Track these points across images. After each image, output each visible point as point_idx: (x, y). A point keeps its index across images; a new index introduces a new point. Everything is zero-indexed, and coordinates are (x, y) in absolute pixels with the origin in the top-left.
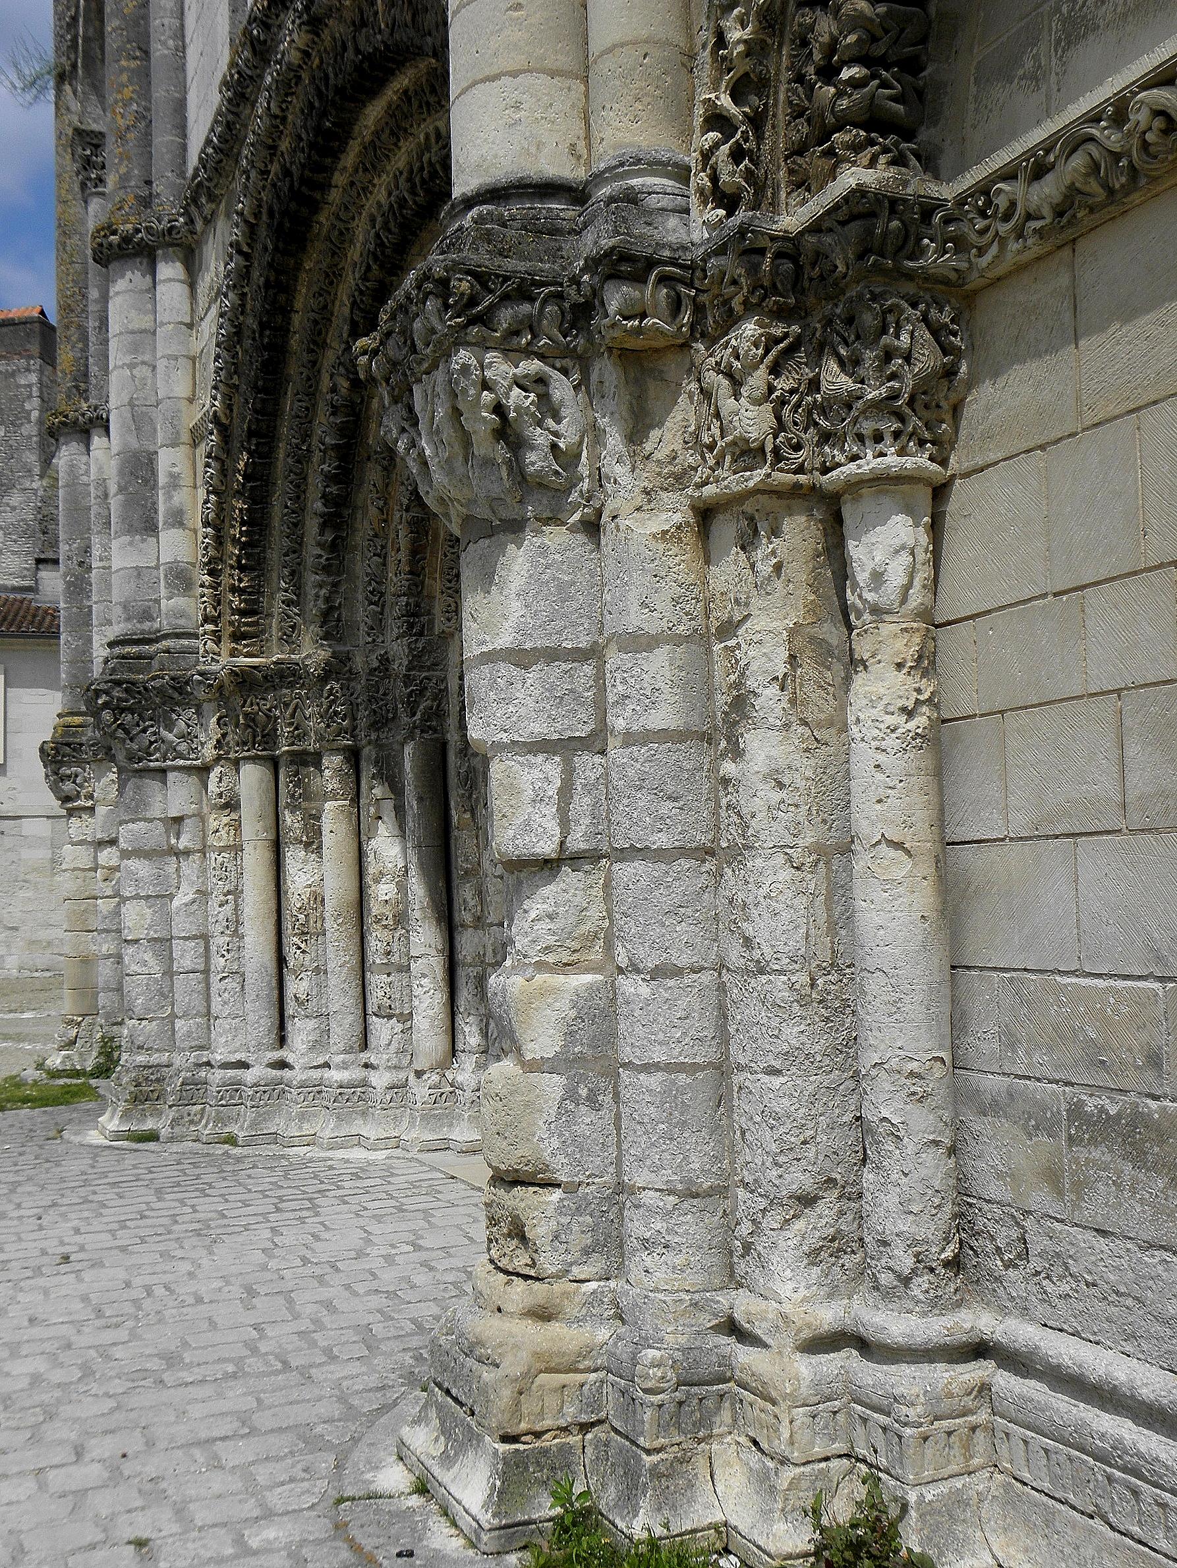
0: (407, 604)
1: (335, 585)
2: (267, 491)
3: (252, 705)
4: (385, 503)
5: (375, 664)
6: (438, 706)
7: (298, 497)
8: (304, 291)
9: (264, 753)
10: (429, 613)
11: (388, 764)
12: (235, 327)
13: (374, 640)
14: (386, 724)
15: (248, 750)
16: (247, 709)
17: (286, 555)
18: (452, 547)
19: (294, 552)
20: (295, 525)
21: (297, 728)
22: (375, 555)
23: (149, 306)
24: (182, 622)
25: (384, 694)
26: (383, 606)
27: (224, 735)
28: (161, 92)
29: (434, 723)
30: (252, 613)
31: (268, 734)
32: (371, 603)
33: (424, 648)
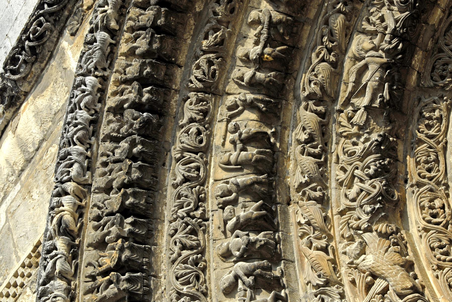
2: (148, 286)
8: (189, 41)
12: (92, 115)
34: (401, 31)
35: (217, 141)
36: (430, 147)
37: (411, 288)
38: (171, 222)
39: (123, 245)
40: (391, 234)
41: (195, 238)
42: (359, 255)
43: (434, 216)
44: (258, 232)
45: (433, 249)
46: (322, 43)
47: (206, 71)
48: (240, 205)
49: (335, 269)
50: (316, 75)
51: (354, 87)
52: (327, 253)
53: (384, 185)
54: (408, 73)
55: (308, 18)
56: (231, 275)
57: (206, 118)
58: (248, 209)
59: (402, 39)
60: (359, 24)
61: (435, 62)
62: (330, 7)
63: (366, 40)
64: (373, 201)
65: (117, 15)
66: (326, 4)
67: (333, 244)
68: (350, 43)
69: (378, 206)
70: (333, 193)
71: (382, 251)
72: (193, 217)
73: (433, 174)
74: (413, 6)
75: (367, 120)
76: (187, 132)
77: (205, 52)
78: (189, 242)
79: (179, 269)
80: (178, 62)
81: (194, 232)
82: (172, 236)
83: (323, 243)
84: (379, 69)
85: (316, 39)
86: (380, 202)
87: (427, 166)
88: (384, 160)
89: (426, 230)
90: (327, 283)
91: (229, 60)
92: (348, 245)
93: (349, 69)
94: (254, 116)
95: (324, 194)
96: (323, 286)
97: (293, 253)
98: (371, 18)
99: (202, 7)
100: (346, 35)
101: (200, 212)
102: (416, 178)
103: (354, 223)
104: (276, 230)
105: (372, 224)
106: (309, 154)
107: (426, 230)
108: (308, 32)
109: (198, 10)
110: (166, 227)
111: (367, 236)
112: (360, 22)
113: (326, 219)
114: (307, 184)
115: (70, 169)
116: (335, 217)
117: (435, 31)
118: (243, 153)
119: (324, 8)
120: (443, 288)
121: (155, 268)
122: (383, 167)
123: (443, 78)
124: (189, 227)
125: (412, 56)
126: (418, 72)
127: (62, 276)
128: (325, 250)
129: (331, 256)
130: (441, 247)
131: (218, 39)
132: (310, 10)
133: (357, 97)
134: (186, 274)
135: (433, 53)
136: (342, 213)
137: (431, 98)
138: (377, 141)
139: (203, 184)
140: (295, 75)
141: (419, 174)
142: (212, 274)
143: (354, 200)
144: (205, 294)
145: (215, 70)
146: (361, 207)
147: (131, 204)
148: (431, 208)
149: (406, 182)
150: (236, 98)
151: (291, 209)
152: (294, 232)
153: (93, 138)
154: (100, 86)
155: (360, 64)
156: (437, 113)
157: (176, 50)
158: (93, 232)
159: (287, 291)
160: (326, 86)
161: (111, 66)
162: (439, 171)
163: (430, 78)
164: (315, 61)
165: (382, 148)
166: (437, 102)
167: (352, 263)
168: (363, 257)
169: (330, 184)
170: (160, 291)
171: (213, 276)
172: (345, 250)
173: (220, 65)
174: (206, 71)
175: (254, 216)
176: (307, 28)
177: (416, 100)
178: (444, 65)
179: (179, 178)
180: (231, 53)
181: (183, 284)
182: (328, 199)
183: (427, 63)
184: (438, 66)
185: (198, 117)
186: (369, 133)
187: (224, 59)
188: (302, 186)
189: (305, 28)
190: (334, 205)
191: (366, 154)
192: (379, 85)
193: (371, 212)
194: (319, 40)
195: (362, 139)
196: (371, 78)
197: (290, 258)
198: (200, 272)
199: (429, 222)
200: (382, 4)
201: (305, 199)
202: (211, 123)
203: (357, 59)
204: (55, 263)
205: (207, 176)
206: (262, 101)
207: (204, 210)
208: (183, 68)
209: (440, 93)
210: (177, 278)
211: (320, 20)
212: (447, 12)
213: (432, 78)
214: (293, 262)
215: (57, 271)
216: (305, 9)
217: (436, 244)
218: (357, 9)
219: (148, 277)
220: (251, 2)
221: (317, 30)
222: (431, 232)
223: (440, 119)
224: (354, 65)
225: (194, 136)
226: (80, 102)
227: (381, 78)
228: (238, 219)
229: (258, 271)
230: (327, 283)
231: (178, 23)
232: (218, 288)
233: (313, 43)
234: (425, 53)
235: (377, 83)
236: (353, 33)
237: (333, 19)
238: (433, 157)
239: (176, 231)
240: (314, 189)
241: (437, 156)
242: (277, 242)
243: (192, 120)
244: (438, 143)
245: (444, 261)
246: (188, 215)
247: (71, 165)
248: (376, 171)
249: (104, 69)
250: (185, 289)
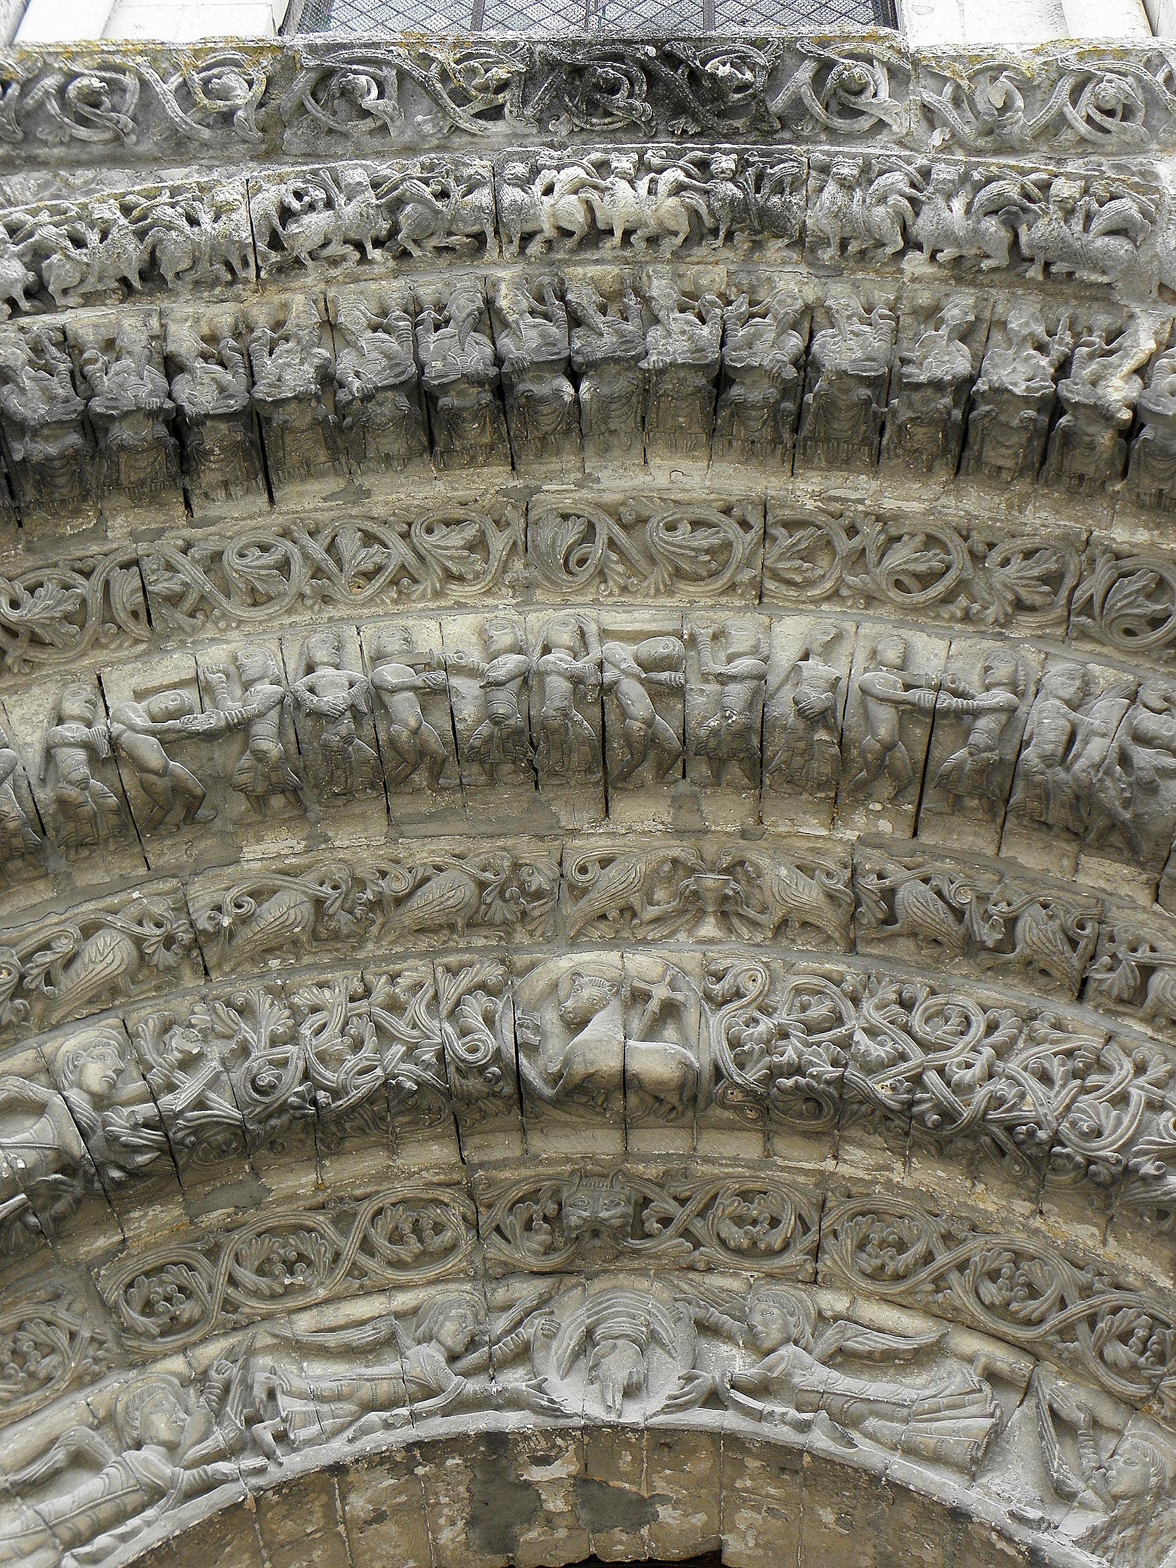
34: (180, 1134)
46: (26, 958)
54: (99, 1226)
55: (69, 876)
59: (168, 1149)
60: (143, 1013)
61: (175, 1264)
62: (134, 910)
63: (109, 1061)
66: (136, 895)
68: (81, 1024)
74: (263, 1115)
84: (47, 1152)
85: (29, 935)
98: (178, 1030)
108: (36, 900)
112: (149, 1010)
117: (257, 1204)
123: (148, 1308)
125: (148, 1201)
126: (124, 1240)
132: (93, 867)
135: (197, 1240)
137: (79, 1321)
155: (39, 1091)
163: (127, 1280)
166: (78, 1341)
176: (42, 892)
177: (50, 1289)
178: (181, 1289)
183: (161, 1244)
184: (165, 1277)
194: (29, 944)
200: (229, 1032)
203: (47, 1071)
209: (106, 1332)
211: (83, 908)
212: (321, 1198)
213: (131, 1285)
216: (85, 853)
218: (179, 978)
220: (15, 698)
221: (54, 919)
224: (28, 1077)
227: (28, 1173)
233: (15, 934)
236: (113, 1013)
237: (108, 939)
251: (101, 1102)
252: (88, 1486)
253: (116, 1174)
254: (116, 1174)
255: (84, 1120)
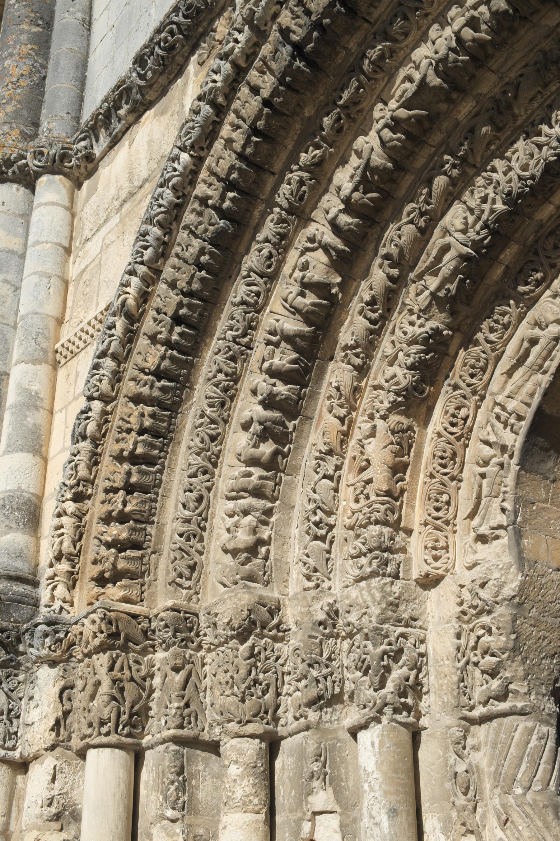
0: (381, 534)
1: (269, 512)
2: (180, 396)
3: (122, 669)
4: (349, 413)
5: (321, 616)
6: (417, 677)
7: (223, 404)
9: (129, 740)
10: (403, 550)
11: (333, 762)
13: (318, 586)
14: (329, 704)
15: (108, 734)
16: (116, 673)
17: (194, 475)
18: (444, 466)
19: (205, 473)
20: (213, 438)
21: (187, 705)
22: (325, 477)
23: (20, 230)
24: (19, 564)
25: (330, 659)
26: (332, 542)
27: (66, 714)
28: (62, 46)
29: (409, 701)
30: (137, 546)
31: (137, 714)
32: (316, 538)
33: (401, 594)
35: (287, 269)
36: (484, 352)
37: (385, 492)
38: (219, 339)
39: (165, 354)
40: (398, 433)
41: (233, 365)
42: (368, 437)
43: (453, 425)
44: (286, 383)
45: (434, 456)
47: (294, 192)
48: (280, 350)
49: (342, 441)
50: (400, 237)
51: (432, 262)
52: (343, 424)
53: (415, 381)
56: (250, 414)
57: (283, 243)
58: (283, 358)
59: (493, 233)
64: (397, 394)
65: (227, 90)
67: (354, 414)
69: (400, 399)
70: (376, 364)
71: (382, 445)
72: (238, 344)
73: (474, 381)
75: (430, 305)
76: (260, 251)
77: (300, 169)
78: (225, 368)
79: (211, 390)
80: (273, 170)
81: (233, 359)
82: (216, 354)
83: (343, 412)
86: (404, 396)
87: (471, 371)
88: (427, 354)
89: (439, 435)
90: (330, 452)
91: (324, 182)
92: (366, 422)
93: (437, 240)
94: (325, 259)
95: (365, 363)
96: (325, 454)
97: (315, 410)
99: (313, 111)
100: (446, 200)
101: (246, 340)
102: (457, 380)
103: (377, 404)
104: (304, 385)
105: (390, 413)
106: (365, 317)
107: (439, 435)
109: (307, 115)
110: (214, 343)
111: (380, 423)
113: (356, 390)
114: (353, 348)
115: (145, 252)
116: (368, 388)
118: (300, 299)
119: (433, 162)
120: (424, 497)
121: (192, 379)
122: (421, 361)
124: (231, 353)
127: (114, 357)
128: (342, 420)
129: (345, 428)
130: (442, 458)
131: (316, 160)
133: (431, 275)
134: (213, 398)
136: (375, 388)
138: (427, 333)
139: (258, 312)
140: (382, 224)
141: (461, 377)
142: (239, 403)
143: (387, 381)
144: (226, 421)
145: (305, 192)
146: (389, 391)
147: (185, 315)
148: (454, 416)
149: (447, 377)
150: (318, 230)
151: (331, 365)
152: (324, 391)
153: (174, 224)
154: (193, 168)
156: (506, 319)
157: (271, 156)
158: (152, 323)
159: (292, 446)
160: (406, 251)
161: (210, 146)
162: (481, 379)
164: (405, 220)
165: (431, 341)
167: (360, 441)
168: (372, 439)
169: (377, 353)
170: (190, 403)
171: (238, 407)
172: (363, 424)
173: (312, 188)
174: (294, 192)
175: (284, 369)
179: (238, 300)
180: (328, 176)
181: (210, 406)
182: (369, 368)
185: (274, 240)
186: (427, 320)
187: (318, 182)
188: (346, 348)
189: (407, 177)
190: (372, 375)
191: (413, 342)
192: (451, 275)
193: (392, 403)
195: (419, 322)
196: (449, 263)
197: (310, 415)
198: (228, 399)
199: (445, 429)
201: (346, 361)
202: (286, 249)
204: (110, 342)
205: (266, 304)
206: (335, 249)
207: (251, 340)
208: (276, 176)
210: (206, 398)
214: (312, 419)
215: (110, 352)
217: (440, 454)
219: (184, 387)
222: (443, 439)
223: (506, 327)
225: (263, 259)
226: (170, 179)
228: (271, 365)
229: (268, 424)
230: (330, 452)
231: (281, 127)
232: (238, 420)
234: (522, 247)
235: (449, 272)
238: (481, 364)
239: (220, 351)
240: (357, 355)
241: (487, 365)
242: (300, 398)
243: (267, 240)
244: (493, 350)
245: (438, 472)
246: (234, 341)
247: (146, 248)
248: (413, 364)
249: (202, 149)
250: (208, 411)
251: (464, 231)
252: (536, 350)
253: (484, 251)
254: (484, 251)
255: (461, 241)
